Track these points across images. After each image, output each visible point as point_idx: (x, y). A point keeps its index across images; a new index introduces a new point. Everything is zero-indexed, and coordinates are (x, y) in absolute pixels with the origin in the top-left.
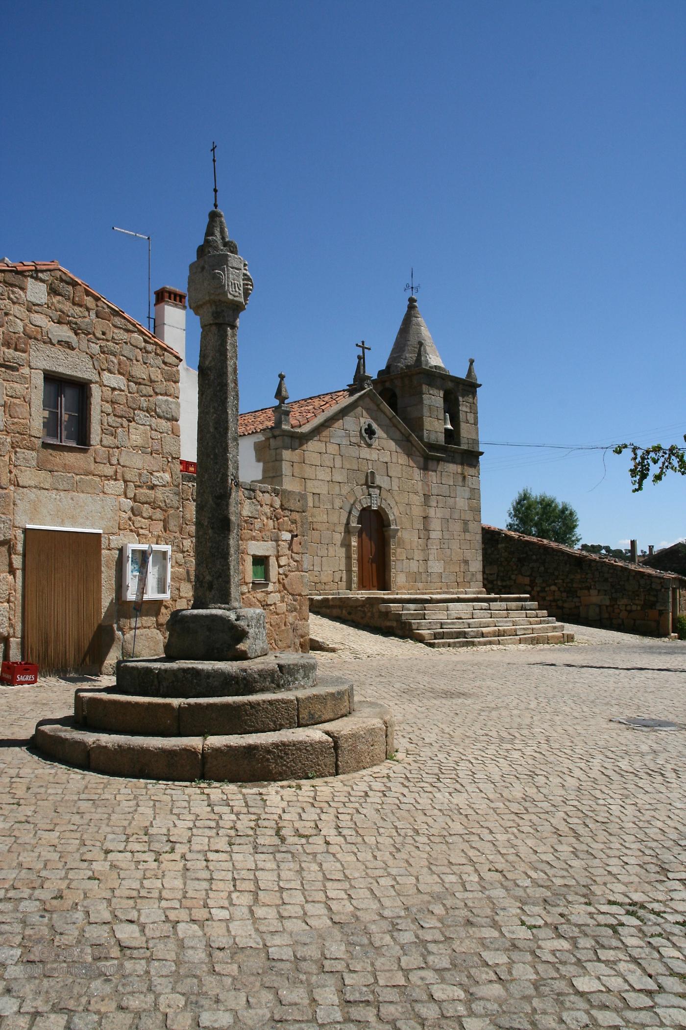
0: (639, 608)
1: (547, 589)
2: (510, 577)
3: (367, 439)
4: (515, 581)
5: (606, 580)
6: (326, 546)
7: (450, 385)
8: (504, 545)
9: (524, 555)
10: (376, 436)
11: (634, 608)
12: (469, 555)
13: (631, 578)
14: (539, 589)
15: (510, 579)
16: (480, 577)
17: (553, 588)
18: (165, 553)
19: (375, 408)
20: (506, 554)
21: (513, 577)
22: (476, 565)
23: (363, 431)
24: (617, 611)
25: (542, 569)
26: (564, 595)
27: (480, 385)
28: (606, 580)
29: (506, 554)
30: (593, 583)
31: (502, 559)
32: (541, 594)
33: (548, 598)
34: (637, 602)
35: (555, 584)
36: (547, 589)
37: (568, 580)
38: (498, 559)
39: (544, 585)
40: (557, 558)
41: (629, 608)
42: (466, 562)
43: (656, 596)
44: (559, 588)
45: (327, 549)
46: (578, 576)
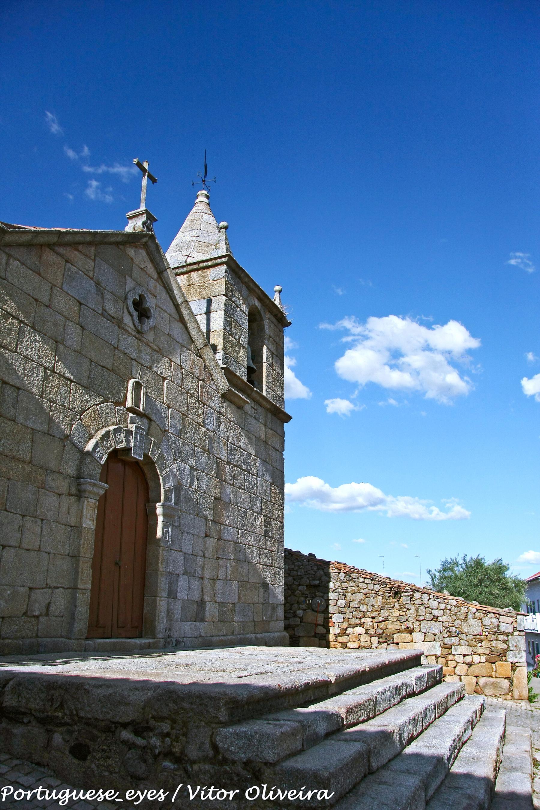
0: (483, 659)
1: (349, 631)
2: (295, 612)
3: (136, 318)
4: (301, 618)
5: (435, 619)
6: (18, 520)
9: (317, 582)
10: (152, 322)
11: (476, 659)
13: (470, 616)
14: (337, 631)
17: (359, 630)
19: (156, 276)
21: (300, 613)
23: (130, 303)
24: (451, 664)
25: (342, 602)
26: (375, 640)
28: (435, 619)
30: (417, 623)
32: (340, 639)
33: (349, 645)
34: (480, 650)
35: (361, 625)
36: (349, 631)
37: (381, 619)
39: (345, 625)
40: (364, 586)
41: (468, 659)
43: (505, 642)
44: (367, 630)
45: (21, 528)
46: (396, 613)
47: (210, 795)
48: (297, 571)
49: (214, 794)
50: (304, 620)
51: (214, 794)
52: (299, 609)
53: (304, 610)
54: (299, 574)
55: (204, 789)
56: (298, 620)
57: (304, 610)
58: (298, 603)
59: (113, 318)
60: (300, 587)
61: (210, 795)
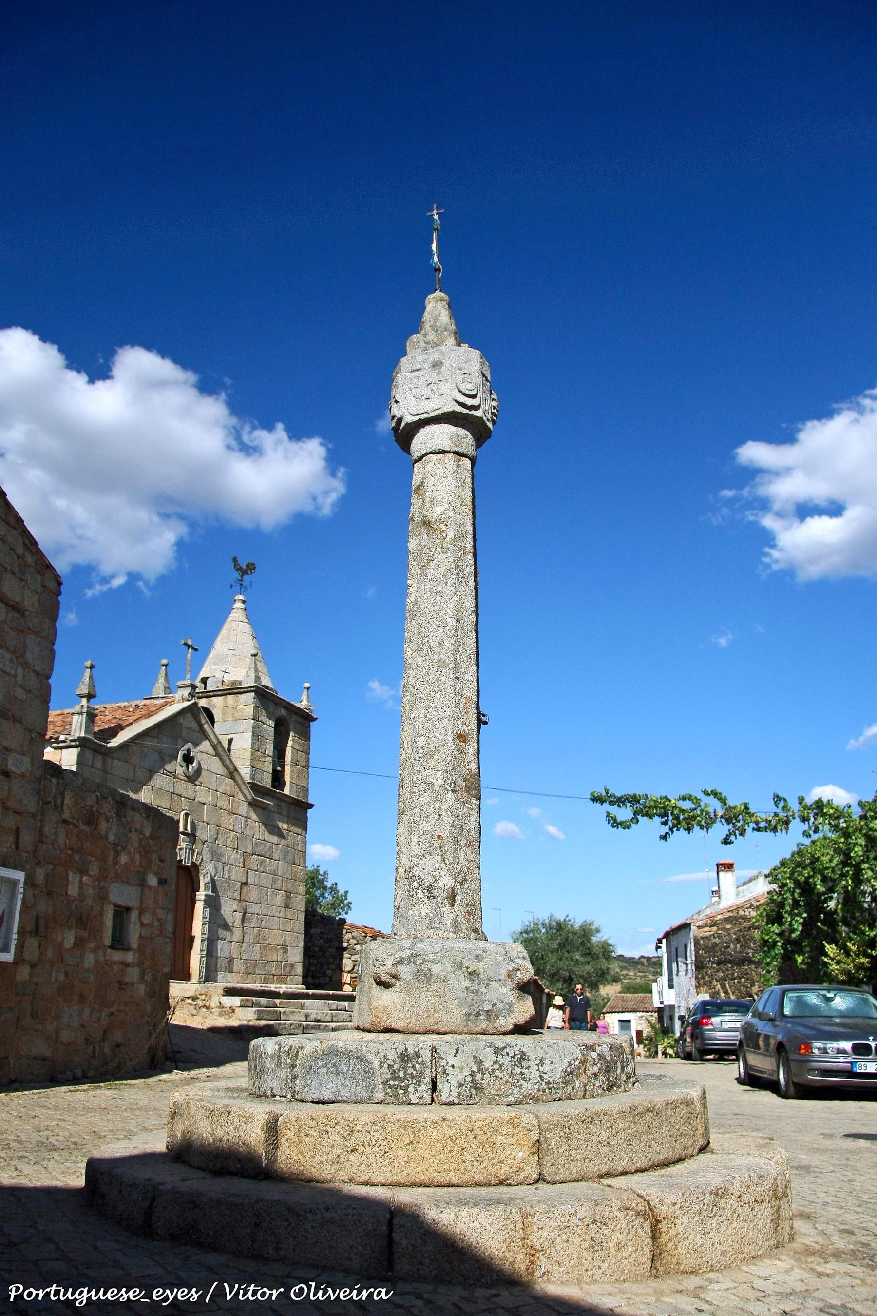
4: (330, 978)
7: (283, 712)
8: (318, 931)
12: (289, 939)
15: (325, 975)
16: (299, 969)
18: (14, 883)
20: (321, 941)
21: (329, 973)
22: (296, 955)
27: (317, 718)
29: (321, 941)
31: (316, 949)
38: (310, 947)
42: (285, 948)
47: (250, 1294)
48: (328, 934)
49: (255, 1293)
50: (333, 979)
51: (255, 1293)
52: (328, 969)
53: (333, 970)
54: (329, 937)
55: (242, 1287)
56: (328, 979)
57: (333, 970)
58: (328, 964)
59: (170, 773)
60: (330, 950)
61: (250, 1294)
